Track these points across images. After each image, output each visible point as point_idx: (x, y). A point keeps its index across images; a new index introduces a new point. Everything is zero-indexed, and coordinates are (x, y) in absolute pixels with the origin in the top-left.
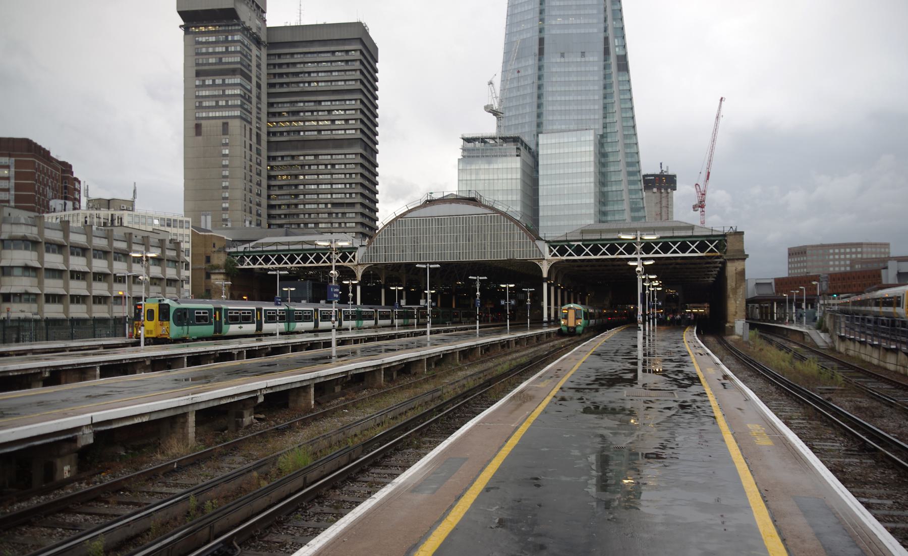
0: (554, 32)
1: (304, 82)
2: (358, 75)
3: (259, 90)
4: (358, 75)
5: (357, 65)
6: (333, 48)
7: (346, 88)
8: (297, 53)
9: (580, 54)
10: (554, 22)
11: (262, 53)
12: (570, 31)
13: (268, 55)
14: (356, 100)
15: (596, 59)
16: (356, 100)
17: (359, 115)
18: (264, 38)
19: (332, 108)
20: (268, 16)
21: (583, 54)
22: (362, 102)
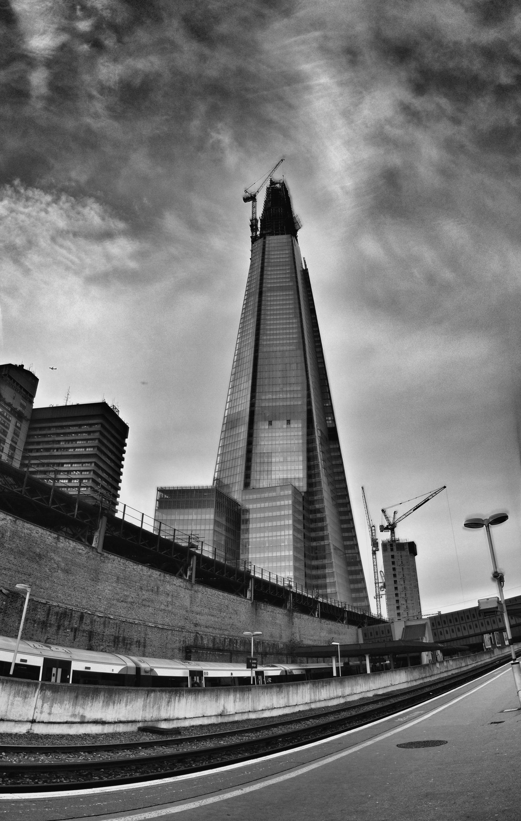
0: (263, 405)
1: (54, 449)
2: (96, 443)
3: (12, 452)
4: (96, 443)
5: (97, 435)
6: (80, 422)
7: (84, 453)
8: (53, 427)
9: (285, 422)
10: (263, 397)
11: (23, 425)
12: (278, 404)
13: (30, 429)
14: (91, 463)
15: (300, 425)
16: (91, 463)
17: (91, 475)
18: (27, 414)
19: (71, 469)
20: (35, 400)
21: (289, 422)
22: (96, 464)
